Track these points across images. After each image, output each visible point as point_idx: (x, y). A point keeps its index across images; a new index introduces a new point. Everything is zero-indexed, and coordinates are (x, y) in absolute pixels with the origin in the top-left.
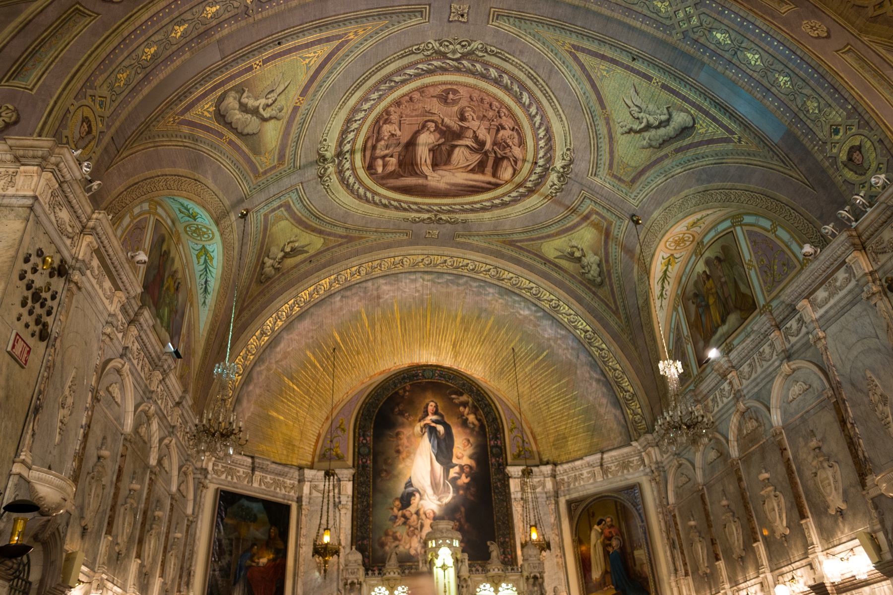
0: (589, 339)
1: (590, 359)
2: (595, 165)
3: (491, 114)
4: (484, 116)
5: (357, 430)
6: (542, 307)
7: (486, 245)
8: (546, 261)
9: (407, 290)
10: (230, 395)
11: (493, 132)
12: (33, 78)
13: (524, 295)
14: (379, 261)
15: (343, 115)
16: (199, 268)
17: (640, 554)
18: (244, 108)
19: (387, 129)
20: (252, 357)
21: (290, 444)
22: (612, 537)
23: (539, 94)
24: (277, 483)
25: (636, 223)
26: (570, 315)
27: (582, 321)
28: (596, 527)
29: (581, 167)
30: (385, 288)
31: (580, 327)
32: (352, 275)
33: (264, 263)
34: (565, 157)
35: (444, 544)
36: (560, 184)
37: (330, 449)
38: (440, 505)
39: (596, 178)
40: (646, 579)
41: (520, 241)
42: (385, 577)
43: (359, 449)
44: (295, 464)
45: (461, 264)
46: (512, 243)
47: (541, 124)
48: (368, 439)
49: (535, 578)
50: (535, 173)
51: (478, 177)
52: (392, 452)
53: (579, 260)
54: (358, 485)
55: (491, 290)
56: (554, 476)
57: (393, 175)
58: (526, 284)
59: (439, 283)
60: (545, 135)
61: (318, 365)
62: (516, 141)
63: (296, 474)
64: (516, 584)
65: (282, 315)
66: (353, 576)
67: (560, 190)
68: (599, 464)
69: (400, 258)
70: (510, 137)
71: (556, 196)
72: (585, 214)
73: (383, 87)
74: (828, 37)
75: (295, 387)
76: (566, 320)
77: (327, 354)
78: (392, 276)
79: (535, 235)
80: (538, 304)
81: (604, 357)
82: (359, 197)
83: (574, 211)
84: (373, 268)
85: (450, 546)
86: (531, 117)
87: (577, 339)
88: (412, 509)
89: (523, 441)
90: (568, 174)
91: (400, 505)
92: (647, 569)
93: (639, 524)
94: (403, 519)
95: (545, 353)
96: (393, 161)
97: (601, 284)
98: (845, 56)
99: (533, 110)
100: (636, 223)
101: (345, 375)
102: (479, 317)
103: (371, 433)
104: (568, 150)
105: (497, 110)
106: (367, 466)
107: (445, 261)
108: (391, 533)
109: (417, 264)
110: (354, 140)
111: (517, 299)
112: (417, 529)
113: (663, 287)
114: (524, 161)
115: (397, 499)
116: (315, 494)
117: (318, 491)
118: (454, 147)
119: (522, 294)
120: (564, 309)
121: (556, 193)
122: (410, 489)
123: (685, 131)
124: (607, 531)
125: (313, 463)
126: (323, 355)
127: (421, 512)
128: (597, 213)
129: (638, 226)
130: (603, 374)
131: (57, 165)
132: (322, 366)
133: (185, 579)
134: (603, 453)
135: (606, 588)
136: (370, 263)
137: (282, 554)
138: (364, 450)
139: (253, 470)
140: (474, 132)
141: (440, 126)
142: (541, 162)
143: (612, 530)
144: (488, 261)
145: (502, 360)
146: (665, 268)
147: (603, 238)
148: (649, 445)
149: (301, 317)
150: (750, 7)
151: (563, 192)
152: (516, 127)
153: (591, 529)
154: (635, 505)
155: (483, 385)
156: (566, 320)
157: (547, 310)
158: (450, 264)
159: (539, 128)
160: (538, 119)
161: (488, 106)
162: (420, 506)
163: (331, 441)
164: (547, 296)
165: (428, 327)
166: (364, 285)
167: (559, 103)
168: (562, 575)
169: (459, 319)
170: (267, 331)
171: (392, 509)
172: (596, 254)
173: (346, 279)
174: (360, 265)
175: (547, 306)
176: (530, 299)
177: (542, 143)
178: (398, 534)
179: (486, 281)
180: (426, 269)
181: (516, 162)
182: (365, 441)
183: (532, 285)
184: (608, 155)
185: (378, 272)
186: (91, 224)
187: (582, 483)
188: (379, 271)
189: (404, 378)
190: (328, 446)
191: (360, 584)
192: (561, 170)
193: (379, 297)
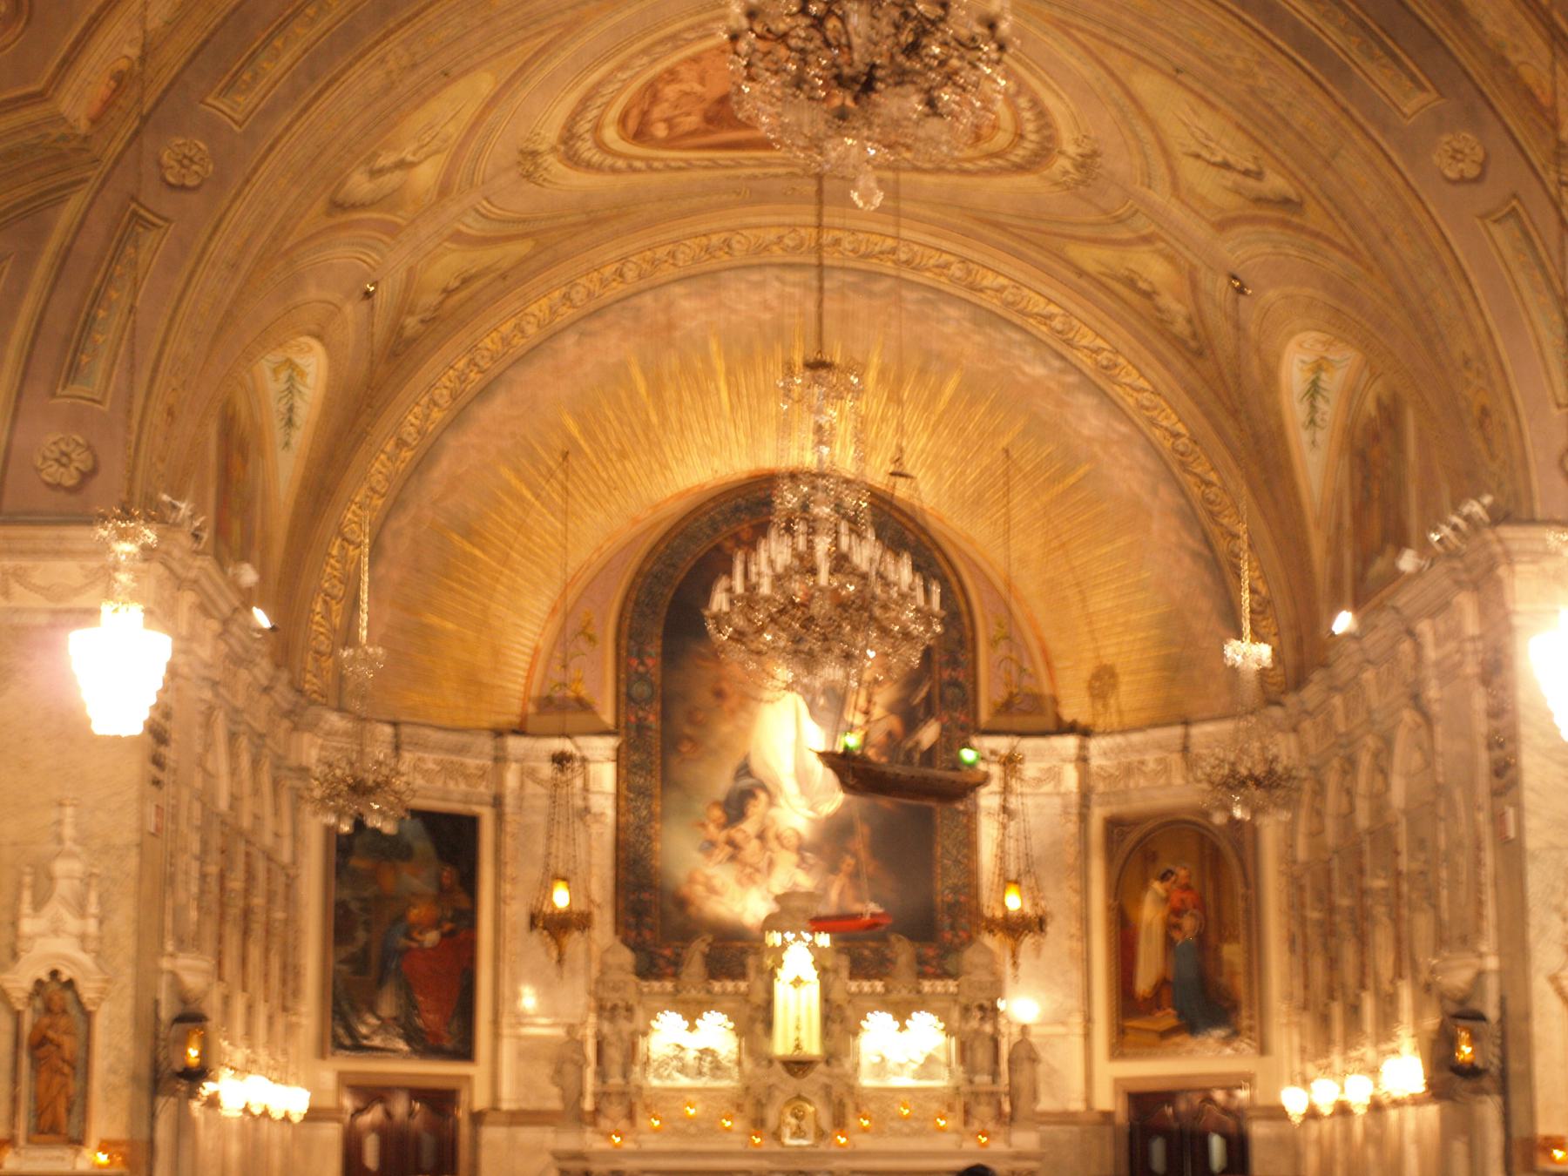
0: (1182, 454)
1: (1183, 501)
5: (623, 642)
6: (1079, 365)
7: (938, 215)
8: (1081, 273)
9: (742, 307)
10: (341, 594)
12: (99, 377)
13: (1034, 331)
14: (670, 247)
15: (572, 98)
16: (273, 387)
17: (1232, 953)
18: (375, 173)
19: (670, 91)
20: (380, 502)
21: (474, 684)
22: (1186, 911)
24: (449, 770)
26: (1141, 390)
27: (1169, 411)
28: (1157, 886)
29: (1119, 163)
30: (687, 305)
31: (1165, 423)
32: (604, 283)
33: (402, 328)
35: (799, 938)
37: (564, 685)
38: (812, 821)
40: (1235, 1007)
41: (1019, 227)
42: (680, 997)
43: (629, 687)
44: (485, 725)
45: (877, 249)
46: (997, 225)
48: (650, 662)
49: (981, 1008)
52: (704, 697)
53: (1148, 295)
54: (629, 772)
55: (952, 312)
56: (1082, 759)
57: (692, 133)
58: (1040, 306)
61: (529, 495)
63: (486, 744)
64: (943, 1016)
65: (441, 395)
66: (617, 995)
68: (1179, 747)
69: (724, 235)
73: (659, 49)
74: (1478, 180)
75: (478, 553)
76: (1131, 401)
77: (549, 469)
78: (704, 278)
79: (1043, 226)
80: (1069, 356)
81: (1212, 503)
82: (614, 170)
85: (813, 947)
87: (1152, 448)
88: (749, 826)
89: (1022, 670)
91: (722, 820)
92: (1240, 984)
93: (1240, 889)
94: (728, 850)
95: (1081, 472)
97: (1199, 353)
98: (1496, 230)
100: (1240, 290)
101: (592, 506)
102: (923, 371)
103: (654, 649)
106: (649, 728)
108: (700, 878)
109: (767, 248)
110: (600, 118)
111: (1017, 336)
112: (758, 870)
113: (1313, 408)
114: (995, 127)
115: (716, 804)
116: (531, 787)
117: (540, 782)
119: (1029, 328)
122: (746, 783)
123: (1285, 202)
124: (1177, 896)
125: (524, 717)
126: (538, 470)
127: (770, 835)
129: (1242, 298)
130: (1207, 541)
131: (168, 553)
132: (538, 496)
133: (291, 984)
134: (1186, 723)
135: (1159, 1014)
136: (648, 253)
137: (467, 919)
138: (640, 689)
139: (397, 748)
143: (1186, 896)
144: (945, 245)
145: (982, 474)
146: (1313, 377)
148: (1277, 727)
149: (484, 393)
150: (1343, 100)
153: (1145, 886)
154: (1238, 846)
155: (934, 524)
156: (1131, 401)
157: (1087, 371)
158: (849, 247)
162: (768, 822)
163: (565, 667)
164: (1087, 339)
166: (635, 301)
168: (1076, 977)
170: (409, 440)
171: (703, 825)
173: (590, 294)
174: (624, 259)
176: (1049, 341)
178: (717, 882)
179: (938, 291)
180: (789, 259)
182: (641, 669)
183: (1053, 309)
185: (667, 272)
186: (192, 574)
187: (1142, 782)
189: (737, 509)
190: (557, 673)
191: (629, 1009)
193: (670, 326)
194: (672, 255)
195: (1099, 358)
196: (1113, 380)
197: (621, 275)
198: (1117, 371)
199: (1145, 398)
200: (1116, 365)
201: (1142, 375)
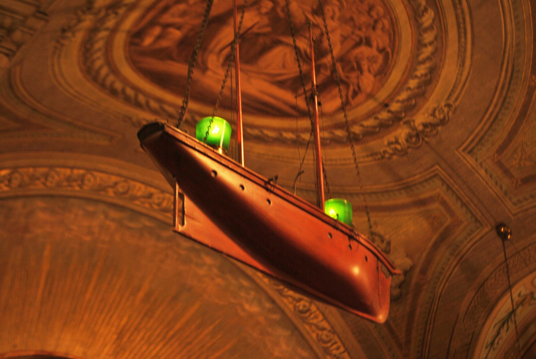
2: (477, 140)
3: (364, 19)
4: (352, 19)
6: (283, 306)
9: (74, 228)
11: (349, 44)
13: (258, 281)
23: (451, 20)
25: (503, 236)
26: (323, 329)
27: (339, 344)
30: (42, 216)
31: (334, 352)
34: (437, 113)
36: (406, 145)
39: (468, 158)
47: (429, 58)
50: (376, 118)
51: (288, 96)
55: (208, 260)
59: (129, 228)
60: (426, 75)
62: (376, 67)
67: (403, 153)
69: (81, 172)
70: (372, 60)
71: (390, 158)
72: (422, 196)
76: (314, 335)
83: (407, 187)
84: (33, 178)
86: (420, 45)
90: (426, 136)
96: (177, 34)
99: (428, 37)
104: (448, 106)
105: (375, 17)
107: (150, 196)
111: (245, 283)
118: (277, 43)
119: (256, 278)
120: (316, 317)
121: (392, 155)
128: (444, 203)
136: (31, 170)
140: (322, 34)
141: (279, 10)
142: (395, 107)
147: (435, 238)
151: (405, 158)
152: (389, 50)
157: (287, 311)
158: (156, 201)
159: (423, 62)
160: (428, 51)
161: (366, 8)
165: (88, 296)
167: (473, 43)
169: (141, 295)
172: (409, 255)
174: (15, 169)
175: (291, 307)
177: (413, 83)
181: (355, 94)
184: (505, 134)
185: (39, 187)
188: (42, 186)
192: (421, 128)
193: (26, 229)
194: (46, 176)
195: (298, 304)
196: (304, 320)
197: (10, 180)
198: (308, 314)
199: (324, 335)
200: (308, 310)
201: (325, 318)
